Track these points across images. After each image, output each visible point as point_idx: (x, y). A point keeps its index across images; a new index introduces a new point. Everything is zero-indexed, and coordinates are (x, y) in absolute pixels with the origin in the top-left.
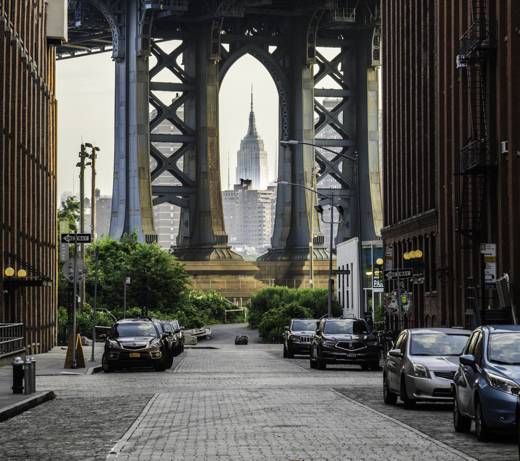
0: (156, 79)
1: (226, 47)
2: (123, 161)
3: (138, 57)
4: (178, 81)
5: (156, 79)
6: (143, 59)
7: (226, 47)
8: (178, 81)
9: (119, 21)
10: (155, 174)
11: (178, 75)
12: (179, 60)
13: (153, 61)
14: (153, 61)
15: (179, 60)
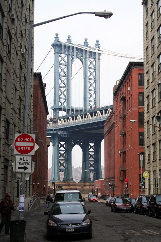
0: (60, 149)
1: (73, 143)
2: (54, 164)
3: (57, 145)
4: (64, 149)
5: (60, 149)
6: (58, 146)
7: (73, 143)
8: (64, 149)
9: (53, 138)
10: (60, 166)
11: (64, 148)
12: (64, 145)
13: (60, 146)
14: (60, 146)
15: (64, 145)
